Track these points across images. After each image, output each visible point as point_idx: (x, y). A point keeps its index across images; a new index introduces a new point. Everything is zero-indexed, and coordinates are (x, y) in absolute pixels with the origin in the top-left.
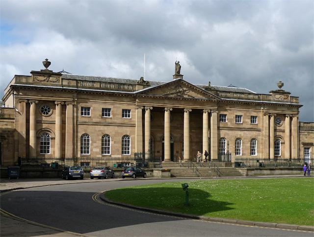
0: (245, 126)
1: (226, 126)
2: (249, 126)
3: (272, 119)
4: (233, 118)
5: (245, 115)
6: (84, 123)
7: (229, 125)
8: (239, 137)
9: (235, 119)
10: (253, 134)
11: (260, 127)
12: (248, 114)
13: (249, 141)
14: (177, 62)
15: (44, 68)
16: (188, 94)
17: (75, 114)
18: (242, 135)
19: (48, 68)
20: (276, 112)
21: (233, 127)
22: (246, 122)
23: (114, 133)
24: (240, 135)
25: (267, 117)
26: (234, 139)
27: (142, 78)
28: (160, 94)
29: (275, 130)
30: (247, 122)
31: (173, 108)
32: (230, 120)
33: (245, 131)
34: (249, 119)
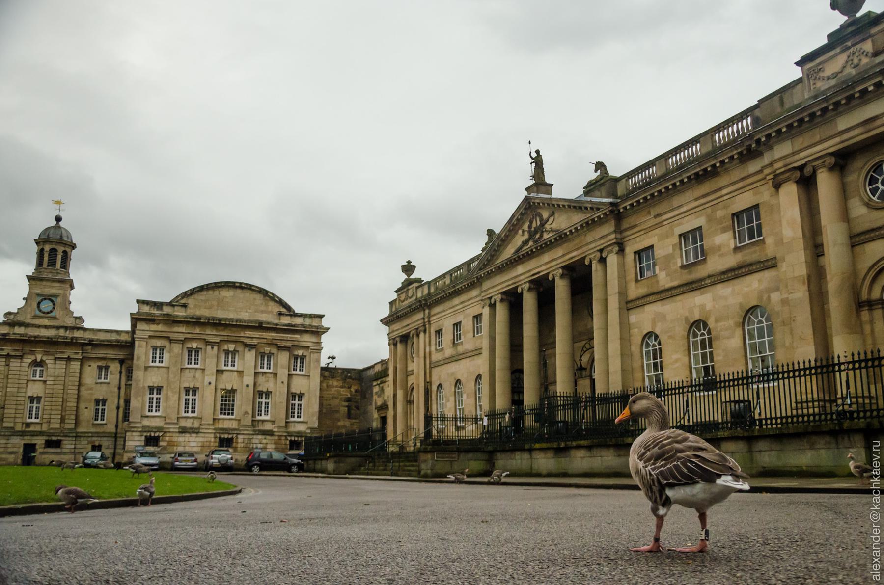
0: (715, 264)
1: (655, 290)
2: (731, 261)
3: (826, 183)
4: (670, 250)
5: (710, 220)
6: (439, 364)
7: (664, 280)
8: (697, 317)
9: (678, 251)
10: (750, 287)
11: (770, 248)
12: (719, 214)
13: (737, 325)
14: (534, 155)
15: (404, 277)
16: (554, 226)
17: (427, 350)
18: (709, 306)
19: (413, 277)
20: (833, 145)
21: (675, 283)
22: (723, 247)
23: (465, 376)
24: (702, 307)
25: (790, 192)
26: (681, 330)
27: (490, 232)
28: (509, 252)
29: (857, 240)
30: (719, 248)
31: (530, 282)
32: (668, 258)
33: (719, 287)
34: (724, 230)
